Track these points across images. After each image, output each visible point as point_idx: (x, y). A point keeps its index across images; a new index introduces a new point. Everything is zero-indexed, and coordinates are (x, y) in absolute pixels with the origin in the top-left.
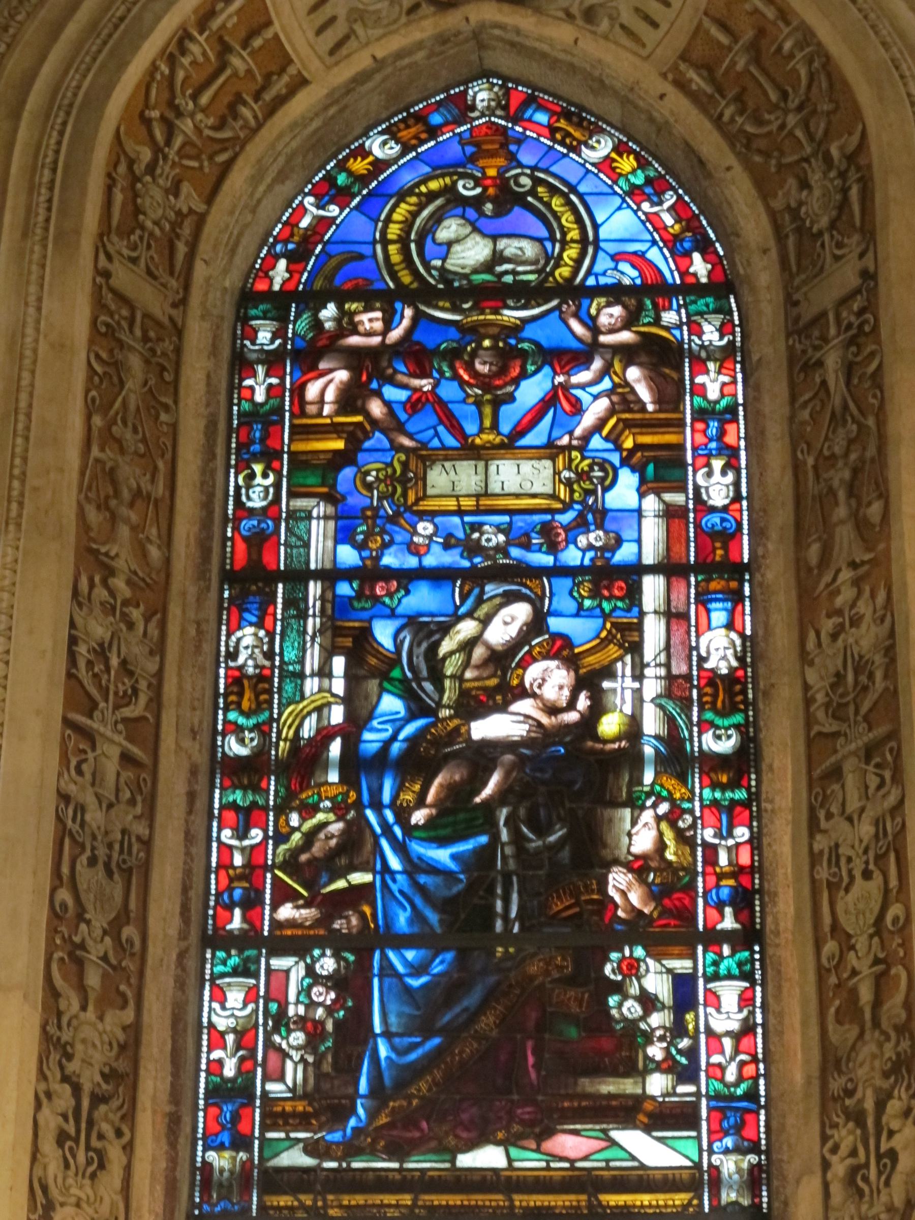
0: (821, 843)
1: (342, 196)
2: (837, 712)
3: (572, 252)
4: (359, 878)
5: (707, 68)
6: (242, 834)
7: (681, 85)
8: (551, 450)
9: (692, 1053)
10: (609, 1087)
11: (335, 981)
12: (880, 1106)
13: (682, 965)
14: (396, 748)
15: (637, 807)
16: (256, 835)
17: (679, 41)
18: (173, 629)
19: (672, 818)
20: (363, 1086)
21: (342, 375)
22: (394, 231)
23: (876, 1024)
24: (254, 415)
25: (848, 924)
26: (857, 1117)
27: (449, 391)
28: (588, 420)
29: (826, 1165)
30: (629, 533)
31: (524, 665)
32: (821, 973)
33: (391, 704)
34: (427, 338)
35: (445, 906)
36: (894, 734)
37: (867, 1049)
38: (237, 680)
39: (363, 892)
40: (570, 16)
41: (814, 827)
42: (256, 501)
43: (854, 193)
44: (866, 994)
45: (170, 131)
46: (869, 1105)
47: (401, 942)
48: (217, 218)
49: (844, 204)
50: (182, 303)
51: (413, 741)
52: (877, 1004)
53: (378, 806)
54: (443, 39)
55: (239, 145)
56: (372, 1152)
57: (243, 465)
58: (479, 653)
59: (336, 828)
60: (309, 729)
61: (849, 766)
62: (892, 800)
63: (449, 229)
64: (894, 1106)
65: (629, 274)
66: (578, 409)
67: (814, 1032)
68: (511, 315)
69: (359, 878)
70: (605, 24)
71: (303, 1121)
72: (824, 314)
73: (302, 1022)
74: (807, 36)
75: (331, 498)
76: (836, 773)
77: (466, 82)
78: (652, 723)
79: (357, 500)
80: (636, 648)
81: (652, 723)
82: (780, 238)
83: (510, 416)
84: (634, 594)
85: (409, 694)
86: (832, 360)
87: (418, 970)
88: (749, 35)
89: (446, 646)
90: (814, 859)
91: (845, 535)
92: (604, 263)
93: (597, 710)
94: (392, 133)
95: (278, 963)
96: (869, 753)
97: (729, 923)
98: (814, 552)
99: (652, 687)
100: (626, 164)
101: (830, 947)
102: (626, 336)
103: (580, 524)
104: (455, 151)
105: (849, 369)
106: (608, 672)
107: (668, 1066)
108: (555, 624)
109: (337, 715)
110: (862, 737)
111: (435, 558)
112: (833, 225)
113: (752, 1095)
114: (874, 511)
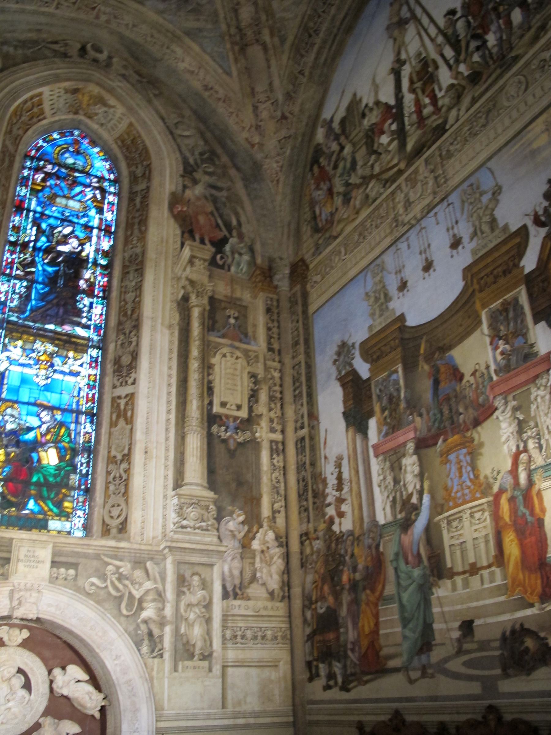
0: (123, 284)
1: (48, 142)
2: (130, 262)
3: (89, 167)
4: (33, 269)
5: (123, 141)
6: (11, 255)
7: (116, 143)
8: (80, 201)
9: (91, 316)
10: (76, 319)
11: (26, 287)
12: (130, 332)
13: (91, 300)
14: (43, 248)
15: (87, 269)
16: (14, 256)
17: (118, 135)
18: (6, 212)
19: (94, 273)
20: (29, 308)
21: (43, 175)
22: (56, 152)
23: (131, 318)
24: (24, 178)
25: (127, 299)
26: (125, 334)
27: (63, 185)
28: (87, 198)
29: (116, 342)
30: (92, 220)
31: (70, 238)
32: (120, 308)
33: (43, 239)
34: (59, 173)
35: (50, 279)
36: (142, 268)
37: (128, 322)
38: (14, 226)
39: (32, 273)
40: (98, 123)
41: (122, 281)
42: (22, 194)
43: (147, 172)
44: (129, 313)
45: (20, 118)
46: (127, 332)
47: (40, 283)
48: (24, 139)
49: (144, 174)
50: (16, 151)
51: (47, 247)
52: (132, 315)
53: (38, 256)
54: (73, 120)
55: (31, 125)
56: (29, 321)
57: (21, 186)
58: (61, 234)
59: (30, 259)
60: (27, 240)
61: (132, 272)
62: (140, 279)
63: (67, 155)
64: (133, 333)
65: (99, 174)
66: (86, 195)
67: (117, 317)
68: (77, 174)
69: (33, 269)
70: (104, 127)
71: (16, 312)
72: (136, 192)
73: (19, 293)
74: (143, 142)
75: (37, 197)
76: (128, 273)
77: (75, 129)
78: (92, 256)
79: (42, 199)
80: (90, 241)
81: (92, 256)
82: (130, 176)
83: (74, 192)
84: (91, 232)
85: (47, 237)
86: (138, 200)
87: (43, 289)
88: (132, 138)
89: (55, 231)
90: (122, 287)
91: (136, 232)
92: (94, 171)
93: (82, 250)
94: (59, 134)
95: (16, 281)
96: (136, 270)
97: (101, 294)
98: (129, 233)
99: (93, 248)
100: (102, 154)
101: (123, 303)
102: (97, 185)
103: (83, 216)
104: (69, 141)
105: (142, 202)
106: (84, 244)
107: (86, 317)
108: (77, 233)
109: (33, 238)
110: (134, 267)
111: (56, 214)
112: (141, 176)
113: (101, 326)
114: (143, 228)
